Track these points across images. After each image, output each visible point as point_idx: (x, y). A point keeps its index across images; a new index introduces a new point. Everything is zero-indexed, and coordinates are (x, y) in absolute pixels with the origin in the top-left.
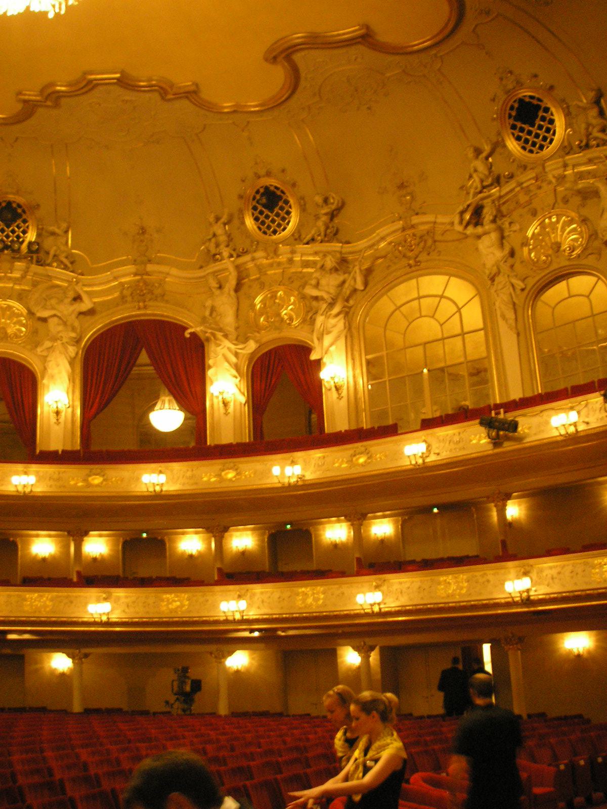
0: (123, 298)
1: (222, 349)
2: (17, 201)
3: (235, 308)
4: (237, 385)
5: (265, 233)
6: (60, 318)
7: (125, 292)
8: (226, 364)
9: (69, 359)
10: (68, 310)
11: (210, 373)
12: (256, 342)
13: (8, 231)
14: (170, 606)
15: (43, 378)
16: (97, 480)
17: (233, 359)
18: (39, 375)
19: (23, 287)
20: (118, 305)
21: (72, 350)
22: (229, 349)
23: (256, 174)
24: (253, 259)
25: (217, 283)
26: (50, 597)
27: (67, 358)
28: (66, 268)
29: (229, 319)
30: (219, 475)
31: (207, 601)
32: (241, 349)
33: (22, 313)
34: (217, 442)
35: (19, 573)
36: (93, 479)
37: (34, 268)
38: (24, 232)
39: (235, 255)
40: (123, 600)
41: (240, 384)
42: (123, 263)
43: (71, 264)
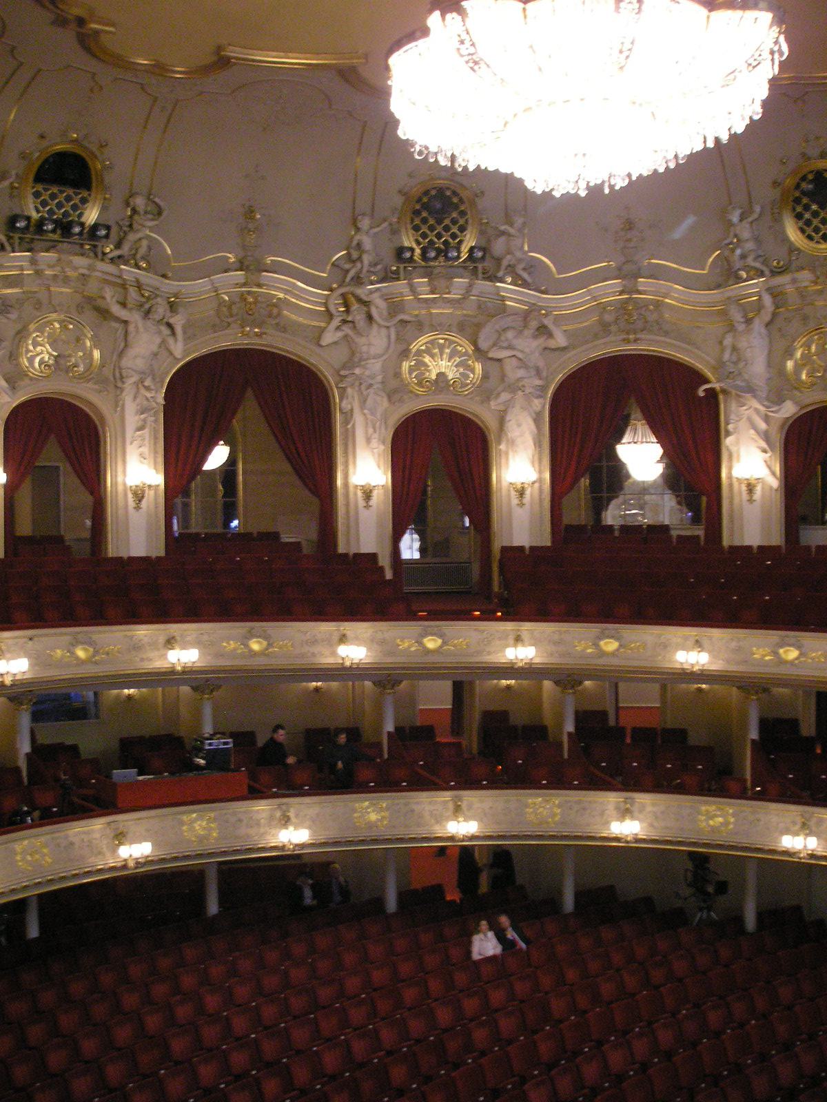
0: (604, 328)
1: (746, 410)
2: (453, 188)
3: (766, 352)
4: (765, 461)
5: (810, 238)
6: (520, 359)
7: (608, 318)
8: (752, 432)
9: (534, 415)
10: (528, 345)
11: (728, 442)
12: (796, 403)
13: (439, 229)
14: (711, 823)
15: (499, 443)
16: (610, 646)
17: (763, 426)
18: (492, 437)
19: (465, 312)
20: (596, 337)
21: (537, 404)
22: (756, 410)
23: (804, 155)
24: (794, 281)
25: (743, 317)
26: (557, 802)
27: (532, 417)
28: (525, 284)
29: (758, 367)
30: (776, 654)
31: (759, 820)
32: (772, 412)
33: (466, 351)
34: (737, 543)
35: (477, 704)
36: (606, 644)
37: (482, 285)
38: (462, 229)
39: (767, 272)
40: (649, 808)
41: (771, 460)
42: (603, 276)
43: (529, 276)
